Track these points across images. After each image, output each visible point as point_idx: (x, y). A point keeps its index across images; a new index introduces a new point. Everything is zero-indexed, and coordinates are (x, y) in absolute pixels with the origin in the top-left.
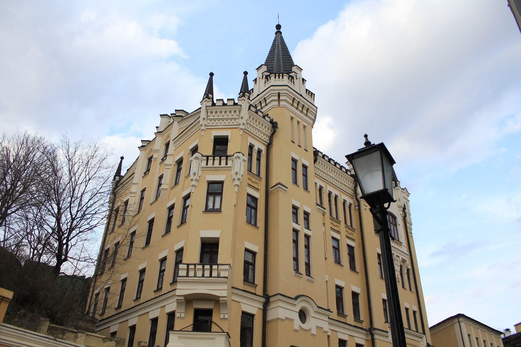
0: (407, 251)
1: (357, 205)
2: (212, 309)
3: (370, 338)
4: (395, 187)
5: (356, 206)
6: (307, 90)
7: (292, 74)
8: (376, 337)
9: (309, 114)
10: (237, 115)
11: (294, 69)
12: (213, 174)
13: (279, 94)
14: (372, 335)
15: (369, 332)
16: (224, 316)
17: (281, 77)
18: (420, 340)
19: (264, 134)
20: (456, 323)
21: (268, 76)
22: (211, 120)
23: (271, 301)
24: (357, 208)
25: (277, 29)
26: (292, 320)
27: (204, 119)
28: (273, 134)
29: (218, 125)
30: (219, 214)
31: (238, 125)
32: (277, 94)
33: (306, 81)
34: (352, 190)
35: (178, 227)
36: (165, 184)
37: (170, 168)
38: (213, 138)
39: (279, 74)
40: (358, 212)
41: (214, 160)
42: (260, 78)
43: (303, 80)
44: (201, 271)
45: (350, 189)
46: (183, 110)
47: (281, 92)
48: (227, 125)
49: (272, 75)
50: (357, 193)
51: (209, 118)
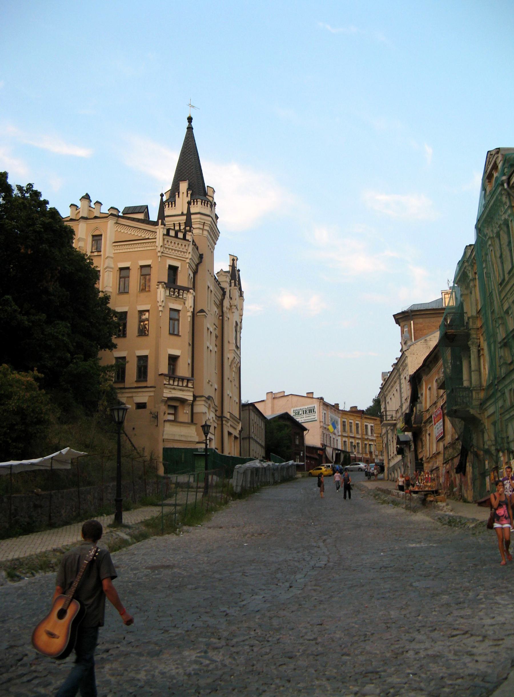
1: (221, 314)
3: (220, 423)
5: (220, 316)
6: (216, 214)
7: (211, 199)
8: (224, 422)
9: (215, 241)
11: (210, 193)
14: (222, 421)
15: (220, 419)
17: (206, 205)
18: (238, 425)
19: (194, 263)
20: (246, 410)
24: (221, 318)
25: (188, 122)
26: (206, 413)
27: (161, 246)
34: (220, 302)
38: (168, 266)
39: (205, 201)
40: (221, 321)
42: (183, 193)
43: (215, 204)
45: (219, 300)
47: (206, 222)
51: (165, 246)
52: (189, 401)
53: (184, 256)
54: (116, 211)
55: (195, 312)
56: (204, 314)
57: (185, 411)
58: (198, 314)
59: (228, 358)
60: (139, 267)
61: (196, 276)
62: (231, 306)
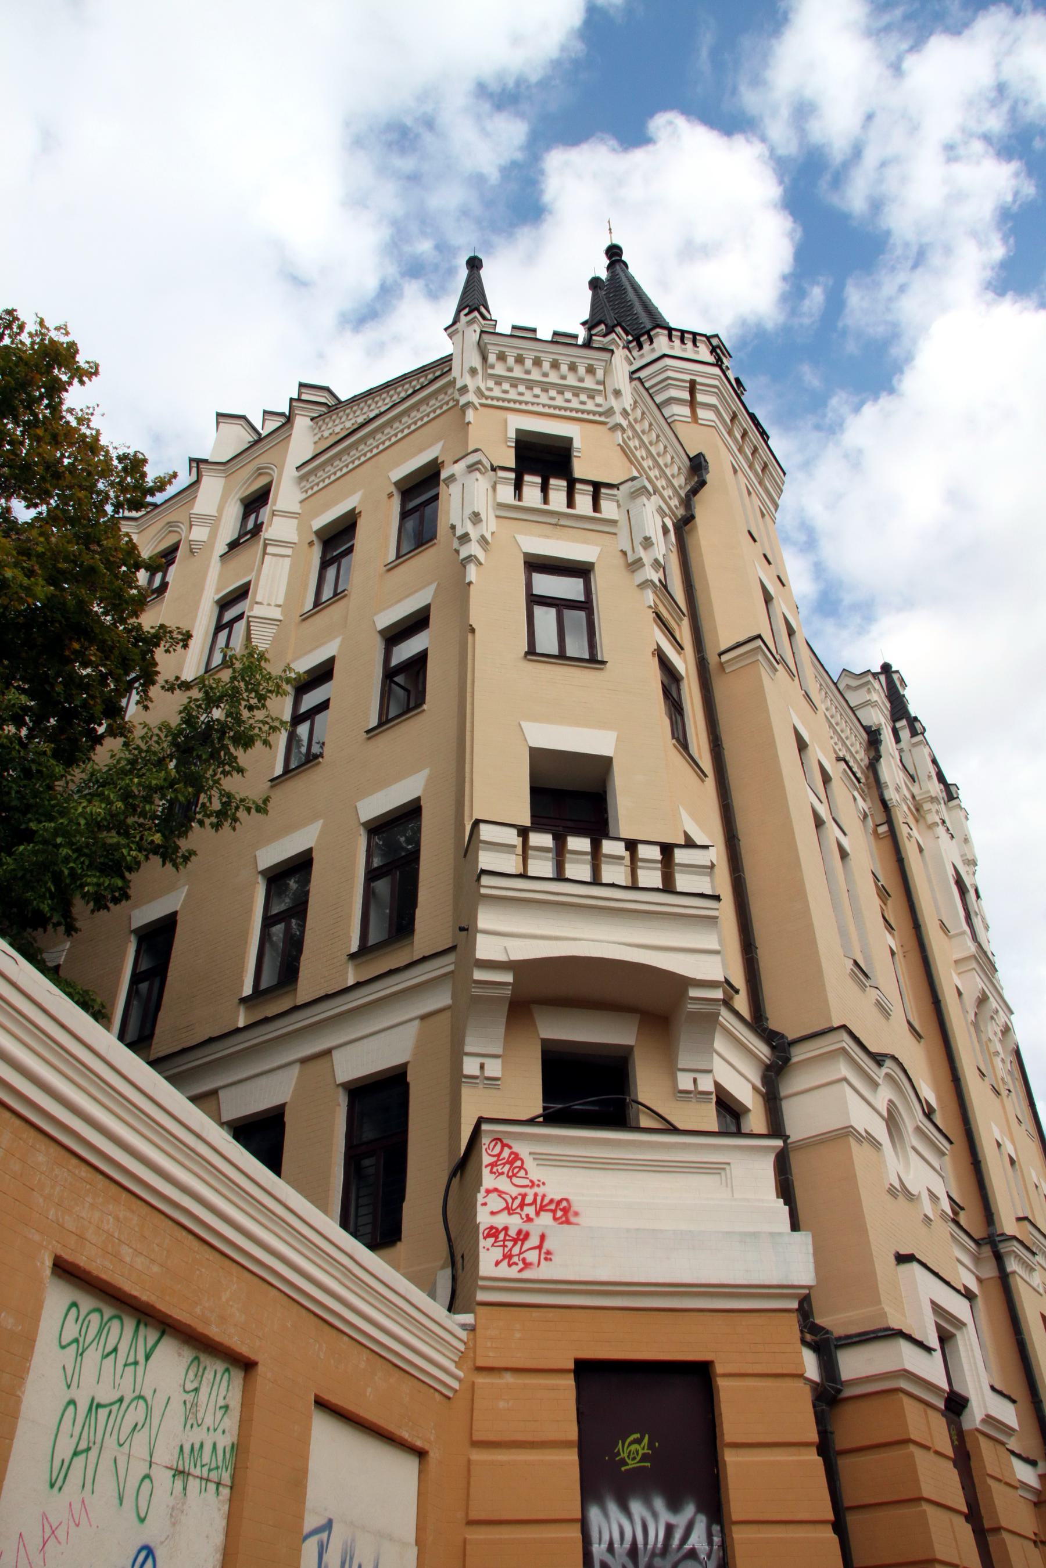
0: (917, 1035)
1: (881, 817)
2: (630, 1049)
3: (990, 1271)
4: (946, 799)
10: (598, 383)
12: (547, 537)
13: (693, 384)
14: (999, 1259)
15: (987, 1251)
16: (695, 1080)
21: (642, 335)
22: (499, 380)
23: (794, 1060)
24: (883, 829)
28: (694, 491)
29: (526, 403)
30: (597, 673)
31: (600, 414)
32: (688, 385)
33: (745, 390)
35: (368, 732)
36: (269, 605)
37: (288, 556)
38: (512, 434)
40: (887, 843)
41: (545, 489)
44: (583, 862)
46: (327, 389)
47: (699, 379)
48: (560, 408)
49: (658, 330)
50: (882, 781)
51: (490, 371)
52: (693, 993)
53: (590, 406)
54: (326, 394)
55: (712, 659)
56: (759, 642)
57: (685, 1082)
58: (724, 658)
59: (960, 994)
60: (393, 489)
61: (690, 543)
62: (917, 810)
